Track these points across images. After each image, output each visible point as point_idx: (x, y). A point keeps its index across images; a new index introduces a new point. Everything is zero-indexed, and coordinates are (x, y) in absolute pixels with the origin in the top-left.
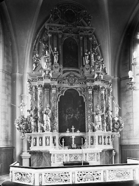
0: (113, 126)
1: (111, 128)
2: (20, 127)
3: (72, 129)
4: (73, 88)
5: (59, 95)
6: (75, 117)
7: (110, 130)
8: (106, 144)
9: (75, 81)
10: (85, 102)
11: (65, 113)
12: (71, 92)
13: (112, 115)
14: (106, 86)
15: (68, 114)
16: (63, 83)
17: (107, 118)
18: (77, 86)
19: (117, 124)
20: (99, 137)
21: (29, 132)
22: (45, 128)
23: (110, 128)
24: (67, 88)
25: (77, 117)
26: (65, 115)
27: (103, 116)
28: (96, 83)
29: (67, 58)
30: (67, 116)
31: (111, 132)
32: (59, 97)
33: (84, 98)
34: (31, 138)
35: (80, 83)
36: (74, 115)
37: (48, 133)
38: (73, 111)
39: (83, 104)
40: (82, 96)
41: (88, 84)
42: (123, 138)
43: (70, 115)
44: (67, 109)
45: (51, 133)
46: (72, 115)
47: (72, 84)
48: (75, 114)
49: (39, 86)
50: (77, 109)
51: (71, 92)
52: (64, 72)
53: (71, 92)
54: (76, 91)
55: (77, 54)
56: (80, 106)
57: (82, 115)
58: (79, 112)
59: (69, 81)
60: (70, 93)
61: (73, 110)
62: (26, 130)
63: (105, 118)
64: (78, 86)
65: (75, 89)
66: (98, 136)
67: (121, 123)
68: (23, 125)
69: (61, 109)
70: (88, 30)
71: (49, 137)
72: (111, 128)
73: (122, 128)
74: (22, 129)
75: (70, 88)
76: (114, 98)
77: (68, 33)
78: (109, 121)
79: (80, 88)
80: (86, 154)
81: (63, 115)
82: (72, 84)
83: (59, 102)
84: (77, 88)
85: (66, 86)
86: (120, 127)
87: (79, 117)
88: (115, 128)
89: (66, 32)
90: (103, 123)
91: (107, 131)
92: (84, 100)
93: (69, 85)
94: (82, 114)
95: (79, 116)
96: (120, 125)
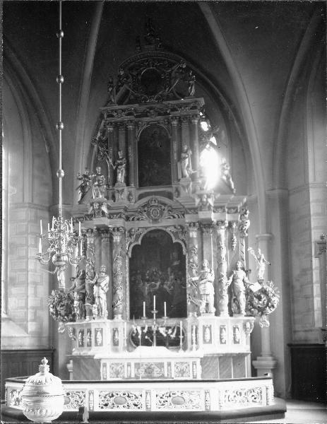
0: (250, 303)
1: (243, 307)
2: (57, 311)
3: (153, 312)
4: (160, 228)
5: (131, 243)
6: (165, 286)
7: (239, 312)
8: (225, 343)
9: (162, 214)
10: (185, 256)
11: (144, 280)
12: (156, 235)
13: (246, 279)
14: (228, 218)
15: (148, 281)
16: (138, 219)
17: (232, 290)
18: (167, 224)
19: (259, 298)
20: (204, 328)
21: (71, 321)
22: (95, 311)
23: (239, 308)
24: (146, 228)
25: (170, 287)
26: (144, 285)
27: (217, 284)
28: (202, 215)
29: (147, 167)
30: (147, 285)
31: (242, 317)
32: (131, 249)
33: (183, 246)
34: (74, 331)
35: (174, 217)
36: (162, 284)
37: (106, 325)
38: (160, 276)
39: (182, 259)
40: (180, 242)
41: (188, 219)
42: (297, 329)
44: (148, 272)
45: (109, 321)
46: (158, 284)
47: (155, 221)
48: (163, 281)
49: (87, 231)
50: (169, 269)
51: (156, 236)
53: (156, 235)
54: (165, 232)
56: (176, 263)
57: (179, 281)
58: (172, 277)
59: (149, 214)
60: (154, 237)
61: (160, 273)
62: (68, 316)
63: (226, 288)
64: (171, 222)
65: (164, 229)
66: (204, 326)
67: (270, 295)
68: (62, 306)
69: (134, 272)
70: (186, 105)
71: (102, 329)
72: (243, 307)
73: (273, 306)
74: (60, 314)
76: (273, 236)
77: (147, 116)
78: (237, 294)
79: (173, 228)
80: (169, 364)
81: (139, 283)
82: (155, 221)
83: (130, 259)
84: (166, 227)
85: (146, 224)
86: (267, 305)
87: (172, 287)
88: (254, 307)
89: (145, 114)
90: (218, 296)
91: (231, 314)
92: (184, 250)
93: (150, 223)
94: (181, 280)
95: (173, 285)
96: (269, 300)
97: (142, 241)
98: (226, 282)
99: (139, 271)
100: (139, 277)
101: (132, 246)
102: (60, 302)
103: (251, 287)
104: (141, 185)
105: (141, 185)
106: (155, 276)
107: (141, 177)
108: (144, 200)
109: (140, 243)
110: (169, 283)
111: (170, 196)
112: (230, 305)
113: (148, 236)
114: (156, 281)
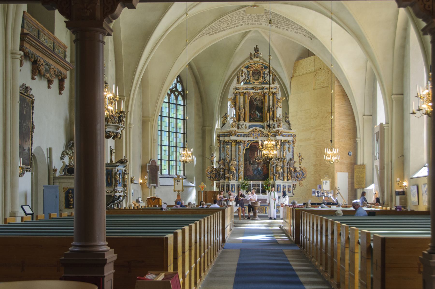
15: (252, 164)
24: (252, 141)
26: (250, 166)
29: (253, 113)
32: (245, 150)
43: (254, 165)
44: (252, 160)
46: (257, 165)
51: (256, 145)
52: (250, 127)
55: (262, 108)
57: (265, 165)
58: (263, 163)
59: (253, 135)
60: (255, 145)
69: (246, 160)
75: (254, 141)
83: (244, 154)
87: (262, 167)
91: (288, 180)
93: (253, 138)
94: (266, 165)
95: (263, 166)
97: (249, 147)
98: (286, 167)
99: (248, 160)
100: (248, 162)
101: (245, 148)
102: (212, 172)
103: (297, 169)
104: (250, 121)
105: (250, 121)
106: (255, 162)
107: (250, 117)
108: (251, 129)
109: (249, 147)
110: (261, 165)
111: (263, 127)
112: (287, 176)
113: (252, 144)
114: (255, 165)
